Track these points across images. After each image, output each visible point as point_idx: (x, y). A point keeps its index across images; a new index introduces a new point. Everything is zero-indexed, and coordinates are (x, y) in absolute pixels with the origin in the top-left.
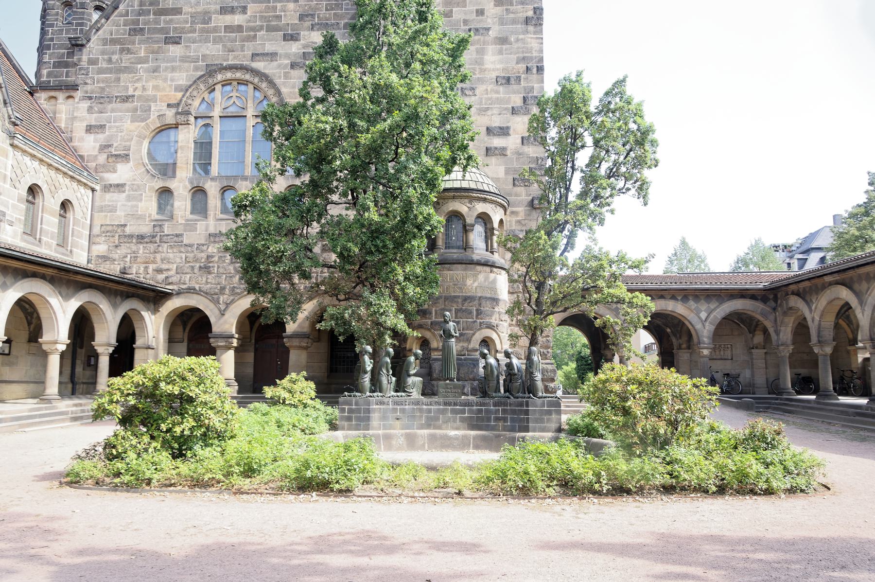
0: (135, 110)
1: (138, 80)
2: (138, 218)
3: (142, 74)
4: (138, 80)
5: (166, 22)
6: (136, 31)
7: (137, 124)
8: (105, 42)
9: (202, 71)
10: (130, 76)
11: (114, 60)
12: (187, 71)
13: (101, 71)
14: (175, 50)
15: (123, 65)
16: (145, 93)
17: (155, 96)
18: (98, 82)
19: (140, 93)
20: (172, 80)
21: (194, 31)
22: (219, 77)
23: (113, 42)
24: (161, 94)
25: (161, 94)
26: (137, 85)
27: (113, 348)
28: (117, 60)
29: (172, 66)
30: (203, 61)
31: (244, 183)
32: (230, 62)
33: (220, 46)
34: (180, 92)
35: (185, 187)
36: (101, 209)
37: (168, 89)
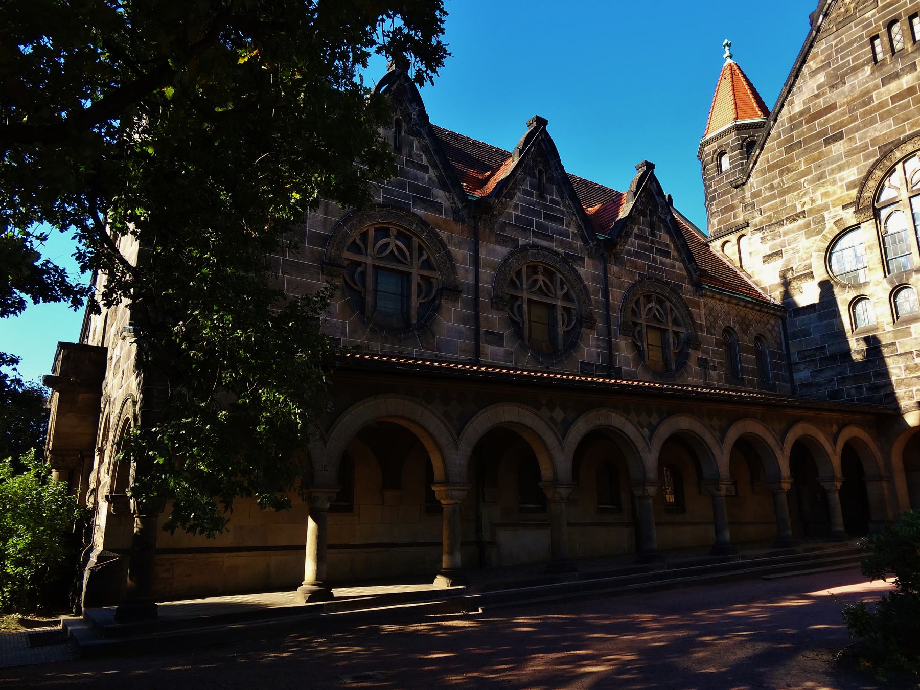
0: (808, 225)
1: (804, 194)
4: (804, 194)
5: (820, 125)
6: (789, 149)
7: (813, 239)
8: (763, 172)
10: (795, 193)
11: (776, 185)
12: (857, 164)
13: (766, 200)
14: (838, 148)
15: (785, 186)
16: (814, 205)
17: (826, 203)
18: (765, 212)
19: (810, 207)
21: (856, 119)
22: (898, 155)
23: (771, 168)
24: (832, 199)
25: (832, 199)
26: (804, 200)
27: (841, 483)
28: (779, 184)
29: (839, 166)
30: (873, 145)
32: (908, 133)
33: (891, 121)
34: (854, 188)
36: (795, 336)
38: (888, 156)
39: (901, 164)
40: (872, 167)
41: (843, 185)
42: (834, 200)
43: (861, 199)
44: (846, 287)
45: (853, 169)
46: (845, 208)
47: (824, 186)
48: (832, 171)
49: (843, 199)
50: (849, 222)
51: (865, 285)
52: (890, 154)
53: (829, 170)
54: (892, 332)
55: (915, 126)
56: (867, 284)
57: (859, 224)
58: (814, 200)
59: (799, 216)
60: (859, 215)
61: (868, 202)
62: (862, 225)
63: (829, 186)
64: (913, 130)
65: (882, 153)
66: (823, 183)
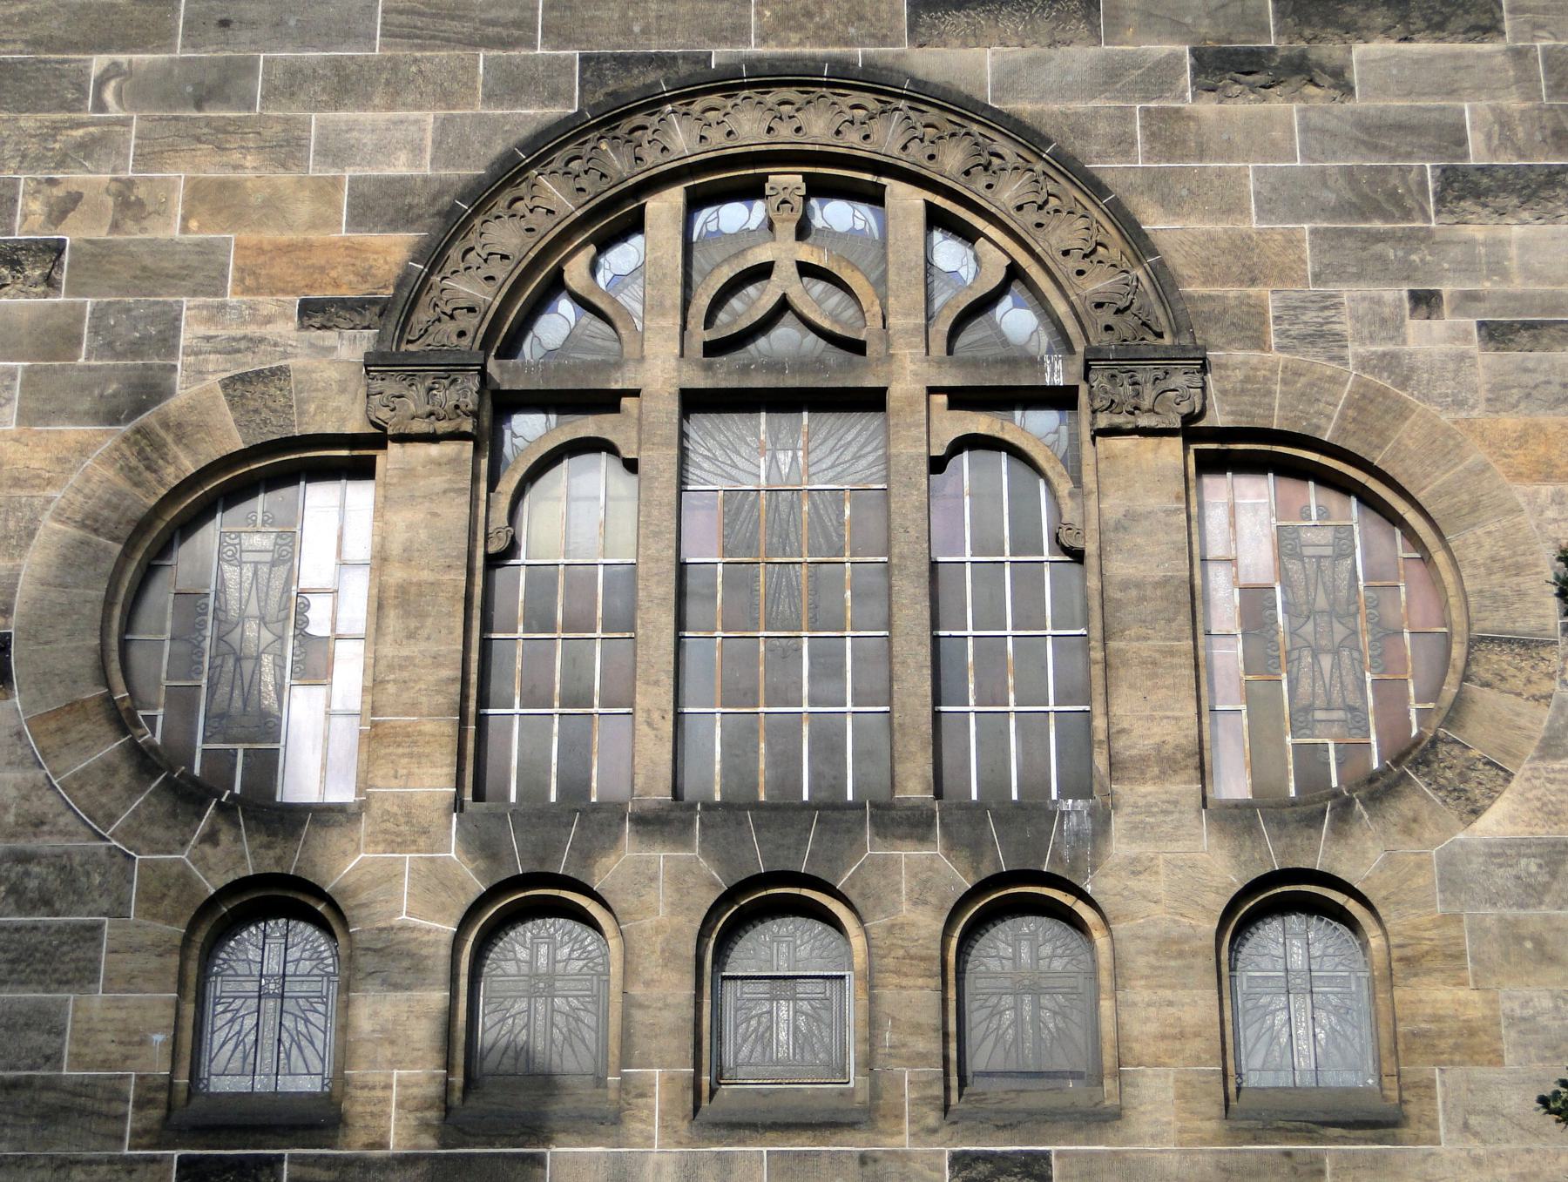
1: (86, 148)
2: (52, 1116)
3: (115, 111)
9: (554, 96)
10: (28, 121)
12: (445, 97)
16: (133, 234)
17: (206, 250)
19: (102, 234)
20: (334, 152)
24: (249, 236)
25: (249, 236)
26: (76, 178)
29: (337, 65)
31: (907, 854)
32: (753, 49)
34: (393, 225)
35: (436, 879)
37: (304, 209)
38: (626, 125)
39: (675, 196)
40: (530, 144)
41: (335, 183)
42: (260, 251)
43: (425, 299)
44: (202, 804)
45: (415, 114)
46: (318, 320)
47: (221, 148)
48: (291, 83)
49: (318, 259)
50: (321, 409)
51: (326, 825)
52: (639, 119)
53: (278, 71)
54: (423, 1167)
55: (800, 28)
56: (341, 817)
57: (379, 439)
58: (140, 203)
59: (15, 265)
60: (391, 386)
61: (462, 334)
62: (390, 458)
63: (250, 161)
64: (781, 44)
65: (599, 96)
66: (223, 129)
